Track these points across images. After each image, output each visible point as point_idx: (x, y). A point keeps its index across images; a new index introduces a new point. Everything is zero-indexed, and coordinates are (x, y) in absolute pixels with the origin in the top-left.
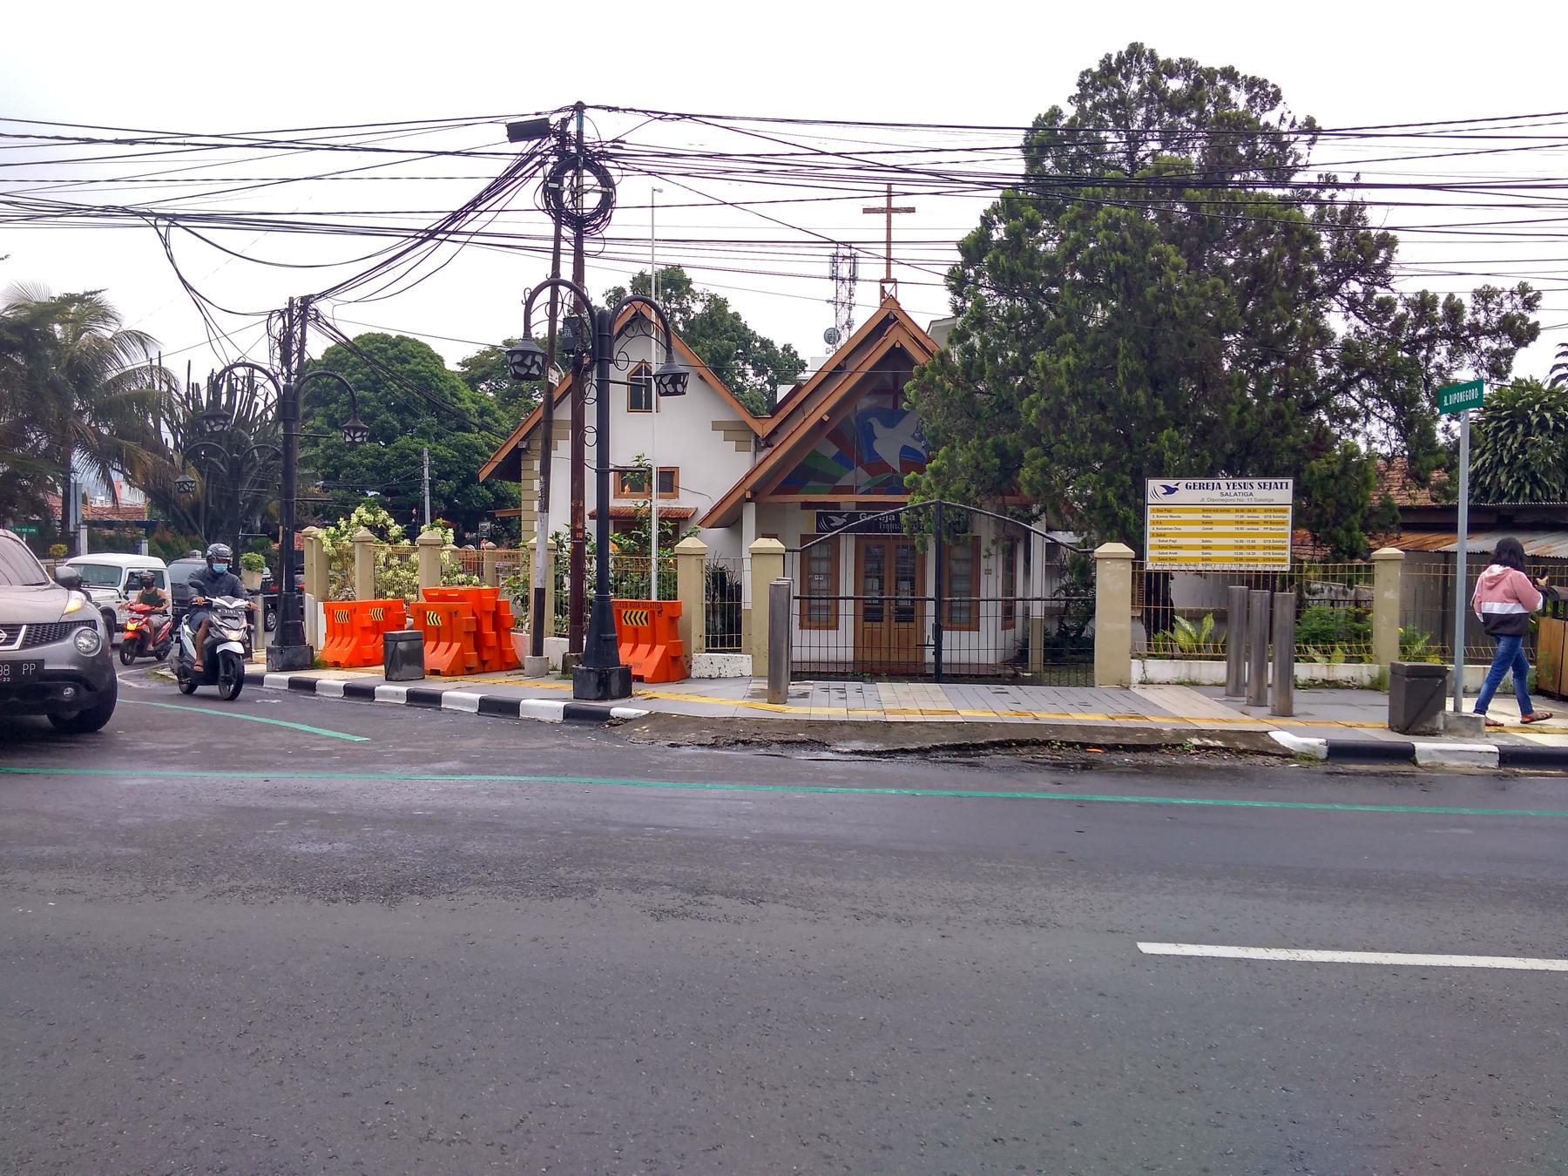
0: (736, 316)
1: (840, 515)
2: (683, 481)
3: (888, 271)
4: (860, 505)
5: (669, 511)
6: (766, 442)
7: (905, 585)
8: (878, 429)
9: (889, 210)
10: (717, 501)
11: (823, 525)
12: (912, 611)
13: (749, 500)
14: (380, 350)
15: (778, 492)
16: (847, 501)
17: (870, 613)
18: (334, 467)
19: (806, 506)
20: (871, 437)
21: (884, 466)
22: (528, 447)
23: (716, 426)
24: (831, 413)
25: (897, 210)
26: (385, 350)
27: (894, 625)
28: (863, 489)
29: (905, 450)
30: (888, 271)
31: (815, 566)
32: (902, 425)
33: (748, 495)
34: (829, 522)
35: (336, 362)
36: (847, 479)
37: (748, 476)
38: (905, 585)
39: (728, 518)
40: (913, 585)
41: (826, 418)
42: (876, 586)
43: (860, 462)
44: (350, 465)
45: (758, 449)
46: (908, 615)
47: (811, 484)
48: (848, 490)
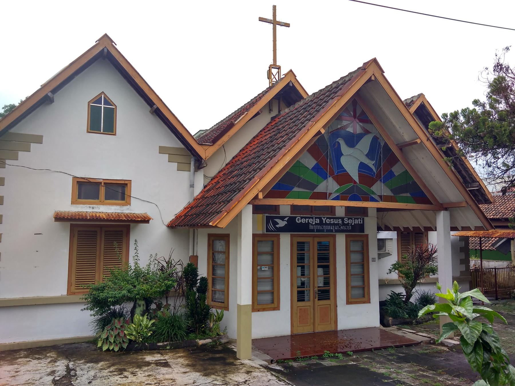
1: (282, 218)
2: (135, 191)
8: (344, 148)
11: (271, 226)
12: (328, 291)
17: (300, 295)
20: (339, 154)
23: (162, 150)
29: (362, 166)
32: (358, 146)
36: (321, 188)
43: (332, 174)
46: (325, 293)
47: (296, 189)
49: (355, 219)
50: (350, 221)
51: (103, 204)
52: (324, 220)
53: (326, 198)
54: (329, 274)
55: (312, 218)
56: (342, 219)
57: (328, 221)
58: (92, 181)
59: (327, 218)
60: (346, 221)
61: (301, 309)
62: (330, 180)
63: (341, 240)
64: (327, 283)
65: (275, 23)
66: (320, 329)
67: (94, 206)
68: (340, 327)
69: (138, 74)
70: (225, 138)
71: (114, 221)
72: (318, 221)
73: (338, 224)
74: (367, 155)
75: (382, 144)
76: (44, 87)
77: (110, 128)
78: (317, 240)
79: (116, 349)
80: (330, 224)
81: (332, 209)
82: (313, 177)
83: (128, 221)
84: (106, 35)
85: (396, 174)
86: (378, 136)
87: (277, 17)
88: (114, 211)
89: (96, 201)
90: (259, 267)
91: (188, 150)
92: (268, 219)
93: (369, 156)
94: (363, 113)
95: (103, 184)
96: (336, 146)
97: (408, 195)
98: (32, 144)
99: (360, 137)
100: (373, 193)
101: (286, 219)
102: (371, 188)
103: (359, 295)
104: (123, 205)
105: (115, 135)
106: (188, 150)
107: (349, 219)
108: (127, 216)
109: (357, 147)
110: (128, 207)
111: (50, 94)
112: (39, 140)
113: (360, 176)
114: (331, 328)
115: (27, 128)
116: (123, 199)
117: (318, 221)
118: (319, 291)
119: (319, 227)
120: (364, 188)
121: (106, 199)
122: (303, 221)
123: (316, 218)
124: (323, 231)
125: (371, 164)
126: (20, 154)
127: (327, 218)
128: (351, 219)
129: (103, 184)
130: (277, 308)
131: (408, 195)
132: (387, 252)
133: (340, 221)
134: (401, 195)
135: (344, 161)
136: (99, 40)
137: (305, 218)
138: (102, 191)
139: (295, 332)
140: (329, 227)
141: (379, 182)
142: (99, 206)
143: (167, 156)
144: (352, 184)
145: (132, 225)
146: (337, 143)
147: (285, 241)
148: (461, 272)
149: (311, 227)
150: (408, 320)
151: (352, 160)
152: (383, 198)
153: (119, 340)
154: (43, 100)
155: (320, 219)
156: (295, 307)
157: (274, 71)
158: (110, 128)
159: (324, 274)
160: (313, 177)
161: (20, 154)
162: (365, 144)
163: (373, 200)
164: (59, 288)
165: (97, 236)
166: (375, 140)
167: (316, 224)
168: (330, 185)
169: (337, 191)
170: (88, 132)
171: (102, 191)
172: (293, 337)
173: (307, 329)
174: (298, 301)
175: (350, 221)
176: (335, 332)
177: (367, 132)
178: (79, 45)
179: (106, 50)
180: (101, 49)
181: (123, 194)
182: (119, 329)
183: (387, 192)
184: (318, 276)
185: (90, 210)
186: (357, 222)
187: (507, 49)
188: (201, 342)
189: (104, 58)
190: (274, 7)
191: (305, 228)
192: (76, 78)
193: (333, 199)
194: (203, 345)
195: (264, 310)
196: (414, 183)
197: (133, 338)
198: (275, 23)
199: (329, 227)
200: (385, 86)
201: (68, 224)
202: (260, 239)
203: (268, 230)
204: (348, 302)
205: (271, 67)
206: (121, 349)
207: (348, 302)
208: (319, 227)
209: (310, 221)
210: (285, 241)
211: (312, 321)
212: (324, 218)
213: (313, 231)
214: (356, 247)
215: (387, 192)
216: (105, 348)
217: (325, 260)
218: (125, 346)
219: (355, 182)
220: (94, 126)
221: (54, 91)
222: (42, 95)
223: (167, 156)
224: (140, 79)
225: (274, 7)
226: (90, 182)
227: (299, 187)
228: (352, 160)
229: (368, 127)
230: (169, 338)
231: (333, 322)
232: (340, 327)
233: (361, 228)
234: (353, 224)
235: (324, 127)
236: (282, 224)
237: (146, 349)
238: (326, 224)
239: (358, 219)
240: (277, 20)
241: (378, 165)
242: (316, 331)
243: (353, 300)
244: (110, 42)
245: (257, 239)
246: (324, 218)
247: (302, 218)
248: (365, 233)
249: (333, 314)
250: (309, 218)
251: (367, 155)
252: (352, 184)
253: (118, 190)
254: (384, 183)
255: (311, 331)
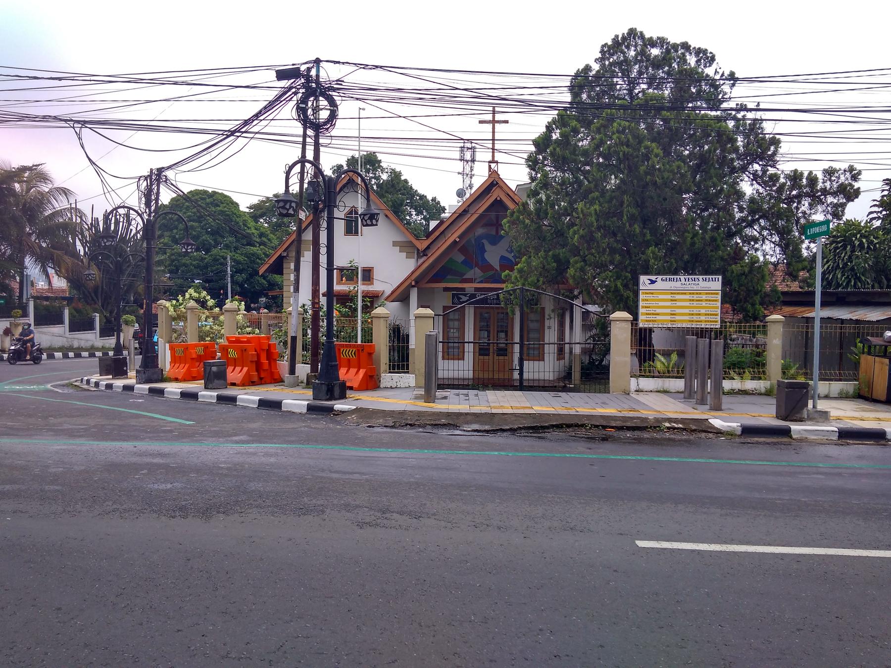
0: (406, 181)
1: (465, 295)
2: (376, 275)
3: (493, 156)
4: (477, 289)
5: (368, 292)
6: (422, 253)
7: (502, 335)
8: (488, 246)
9: (494, 122)
10: (395, 286)
11: (456, 300)
13: (413, 286)
14: (202, 199)
15: (429, 282)
16: (469, 287)
17: (482, 351)
18: (175, 266)
19: (446, 289)
20: (483, 250)
21: (491, 267)
22: (288, 255)
23: (395, 244)
24: (460, 237)
25: (499, 122)
26: (204, 199)
27: (496, 358)
28: (478, 280)
30: (493, 156)
31: (451, 324)
33: (413, 283)
34: (459, 299)
35: (177, 206)
37: (413, 273)
38: (502, 335)
39: (401, 296)
40: (506, 335)
41: (458, 240)
42: (486, 336)
44: (185, 265)
45: (419, 257)
46: (504, 352)
47: (449, 277)
48: (470, 281)
65: (494, 122)
135: (486, 256)
149: (489, 301)
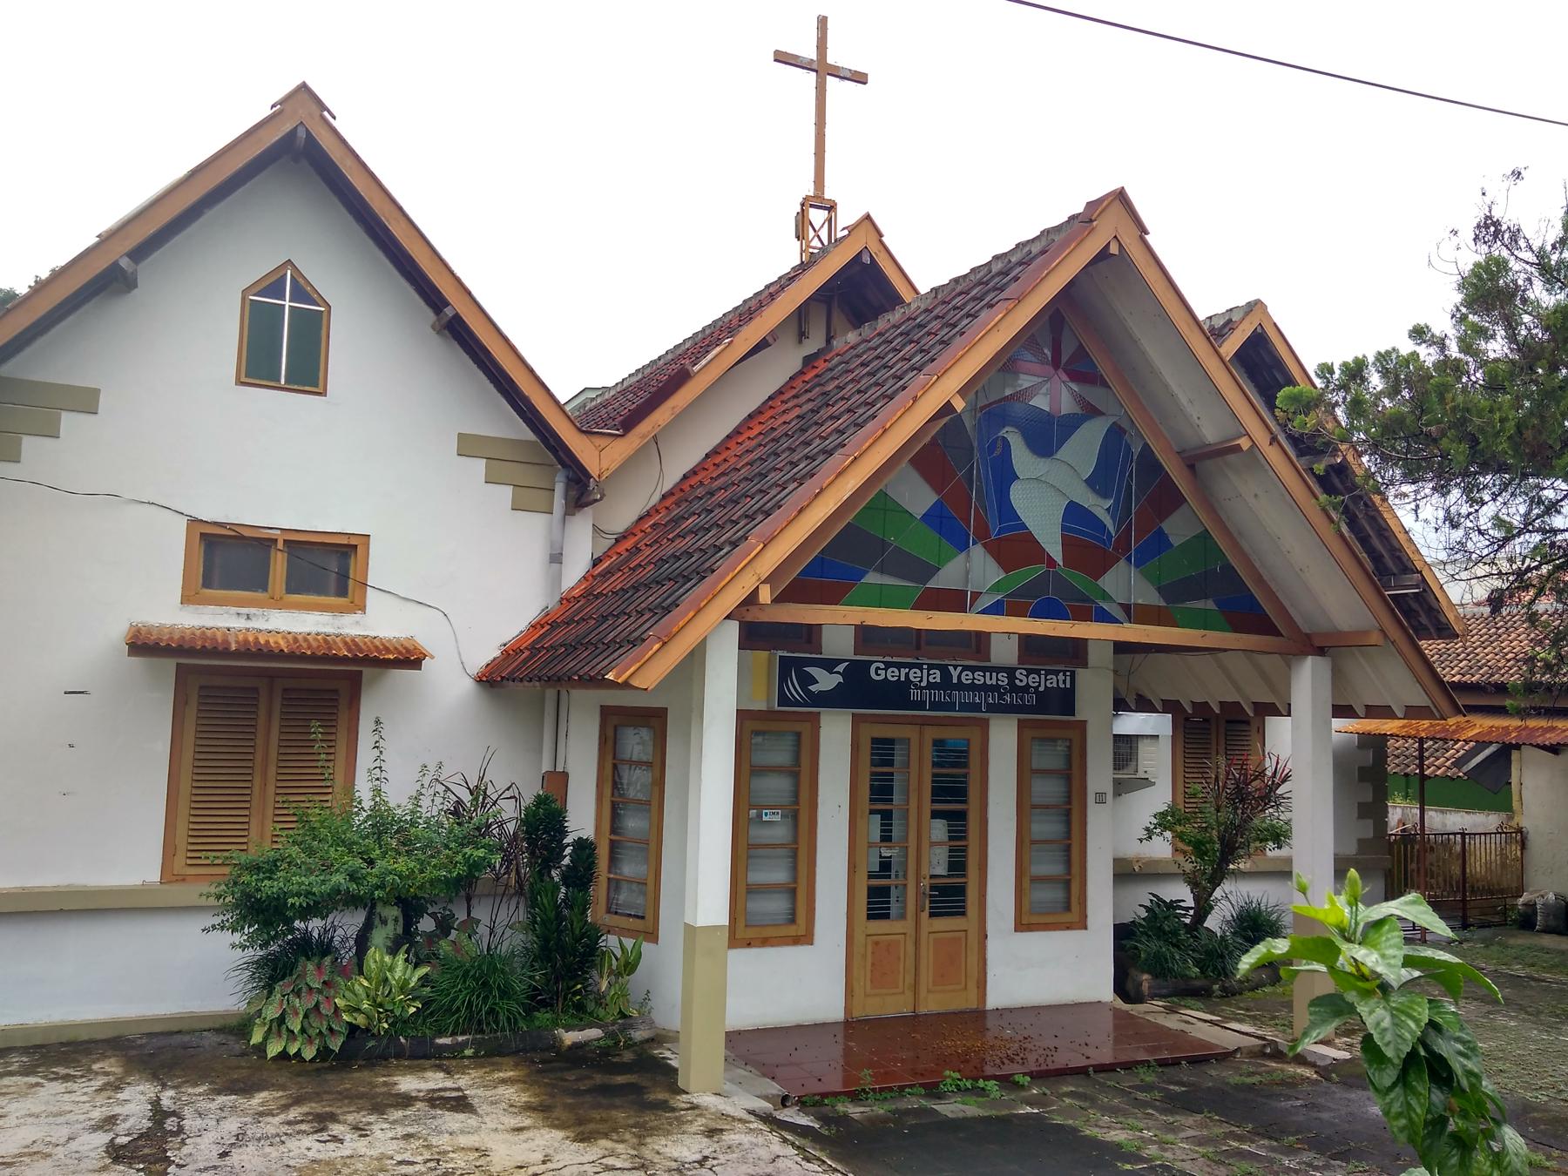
1: (829, 665)
2: (380, 568)
7: (939, 830)
8: (1022, 458)
11: (794, 689)
12: (961, 891)
17: (877, 901)
20: (1005, 475)
23: (468, 446)
28: (987, 601)
29: (1074, 513)
32: (1064, 453)
36: (948, 577)
43: (982, 535)
46: (951, 897)
47: (872, 578)
49: (1048, 672)
50: (1033, 680)
51: (278, 604)
52: (955, 674)
53: (962, 608)
54: (964, 838)
55: (920, 666)
56: (1011, 672)
57: (967, 678)
58: (247, 533)
59: (965, 668)
60: (1022, 679)
61: (877, 943)
62: (977, 552)
63: (1003, 738)
64: (957, 864)
65: (822, 69)
66: (932, 1004)
67: (252, 611)
68: (994, 1000)
69: (400, 209)
70: (661, 416)
71: (313, 658)
72: (936, 676)
73: (996, 688)
74: (1090, 482)
75: (1136, 450)
76: (106, 239)
77: (308, 375)
78: (931, 733)
79: (309, 1053)
80: (973, 687)
81: (979, 642)
82: (924, 543)
83: (355, 660)
84: (304, 88)
85: (1176, 541)
86: (1125, 425)
87: (829, 52)
88: (313, 629)
89: (259, 595)
90: (753, 812)
91: (545, 448)
92: (786, 665)
93: (1098, 482)
94: (1081, 353)
95: (280, 545)
96: (998, 452)
97: (1210, 605)
98: (64, 415)
99: (1069, 425)
100: (1106, 596)
101: (840, 668)
102: (1100, 582)
103: (1053, 903)
104: (342, 610)
105: (323, 394)
106: (545, 448)
107: (1030, 672)
108: (351, 644)
109: (1058, 456)
110: (358, 616)
111: (125, 263)
112: (86, 401)
113: (1067, 543)
114: (967, 1002)
115: (50, 365)
116: (342, 591)
117: (936, 676)
118: (933, 888)
119: (939, 695)
120: (1077, 579)
121: (289, 591)
122: (892, 675)
123: (931, 667)
124: (949, 706)
125: (1100, 507)
126: (29, 444)
127: (965, 668)
128: (1038, 672)
129: (280, 545)
130: (806, 938)
131: (1210, 605)
132: (1141, 775)
133: (1003, 680)
134: (1189, 604)
135: (1019, 496)
136: (281, 102)
137: (899, 666)
138: (279, 565)
139: (858, 1013)
140: (969, 697)
141: (1122, 563)
142: (266, 612)
143: (481, 464)
144: (1039, 569)
145: (367, 672)
146: (999, 443)
147: (836, 735)
148: (1359, 841)
149: (915, 694)
150: (1198, 983)
151: (1043, 496)
152: (1134, 613)
153: (318, 1025)
154: (106, 278)
155: (946, 674)
156: (859, 938)
157: (817, 216)
158: (308, 375)
159: (951, 838)
160: (924, 543)
161: (29, 444)
162: (1083, 448)
163: (1104, 617)
164: (137, 862)
165: (259, 706)
166: (1115, 435)
167: (930, 686)
168: (976, 568)
169: (996, 588)
170: (239, 382)
171: (279, 565)
172: (851, 1026)
173: (894, 1005)
174: (870, 917)
175: (1033, 680)
176: (979, 1015)
177: (1091, 412)
178: (222, 113)
179: (301, 134)
180: (288, 127)
181: (343, 577)
182: (320, 991)
183: (1146, 595)
184: (933, 844)
185: (238, 624)
186: (1053, 682)
187: (1517, 175)
188: (570, 1037)
189: (298, 157)
190: (822, 22)
191: (896, 695)
192: (209, 215)
193: (983, 612)
194: (577, 1046)
195: (765, 942)
196: (1229, 569)
197: (361, 1020)
198: (822, 69)
199: (969, 697)
200: (1150, 275)
201: (169, 665)
202: (759, 726)
203: (784, 700)
204: (1021, 926)
205: (806, 204)
206: (324, 1053)
207: (1021, 926)
208: (939, 695)
209: (914, 675)
210: (836, 735)
211: (910, 979)
212: (955, 667)
213: (920, 705)
214: (1048, 758)
215: (1146, 595)
216: (273, 1049)
217: (955, 796)
218: (336, 1044)
219: (1051, 562)
220: (257, 367)
221: (140, 253)
222: (100, 265)
223: (481, 464)
224: (403, 223)
225: (822, 22)
226: (242, 537)
227: (882, 570)
228: (1043, 496)
229: (1094, 395)
230: (472, 1023)
231: (972, 985)
232: (994, 1000)
233: (1065, 700)
234: (1042, 689)
235: (962, 392)
236: (826, 681)
237: (398, 1056)
238: (960, 686)
239: (1056, 673)
240: (830, 60)
241: (1121, 512)
242: (923, 1010)
243: (1034, 920)
244: (314, 108)
245: (750, 725)
246: (955, 667)
247: (888, 665)
248: (1078, 717)
249: (973, 959)
250: (910, 666)
251: (1090, 482)
252: (1039, 569)
253: (330, 565)
254: (1137, 566)
255: (906, 1011)
